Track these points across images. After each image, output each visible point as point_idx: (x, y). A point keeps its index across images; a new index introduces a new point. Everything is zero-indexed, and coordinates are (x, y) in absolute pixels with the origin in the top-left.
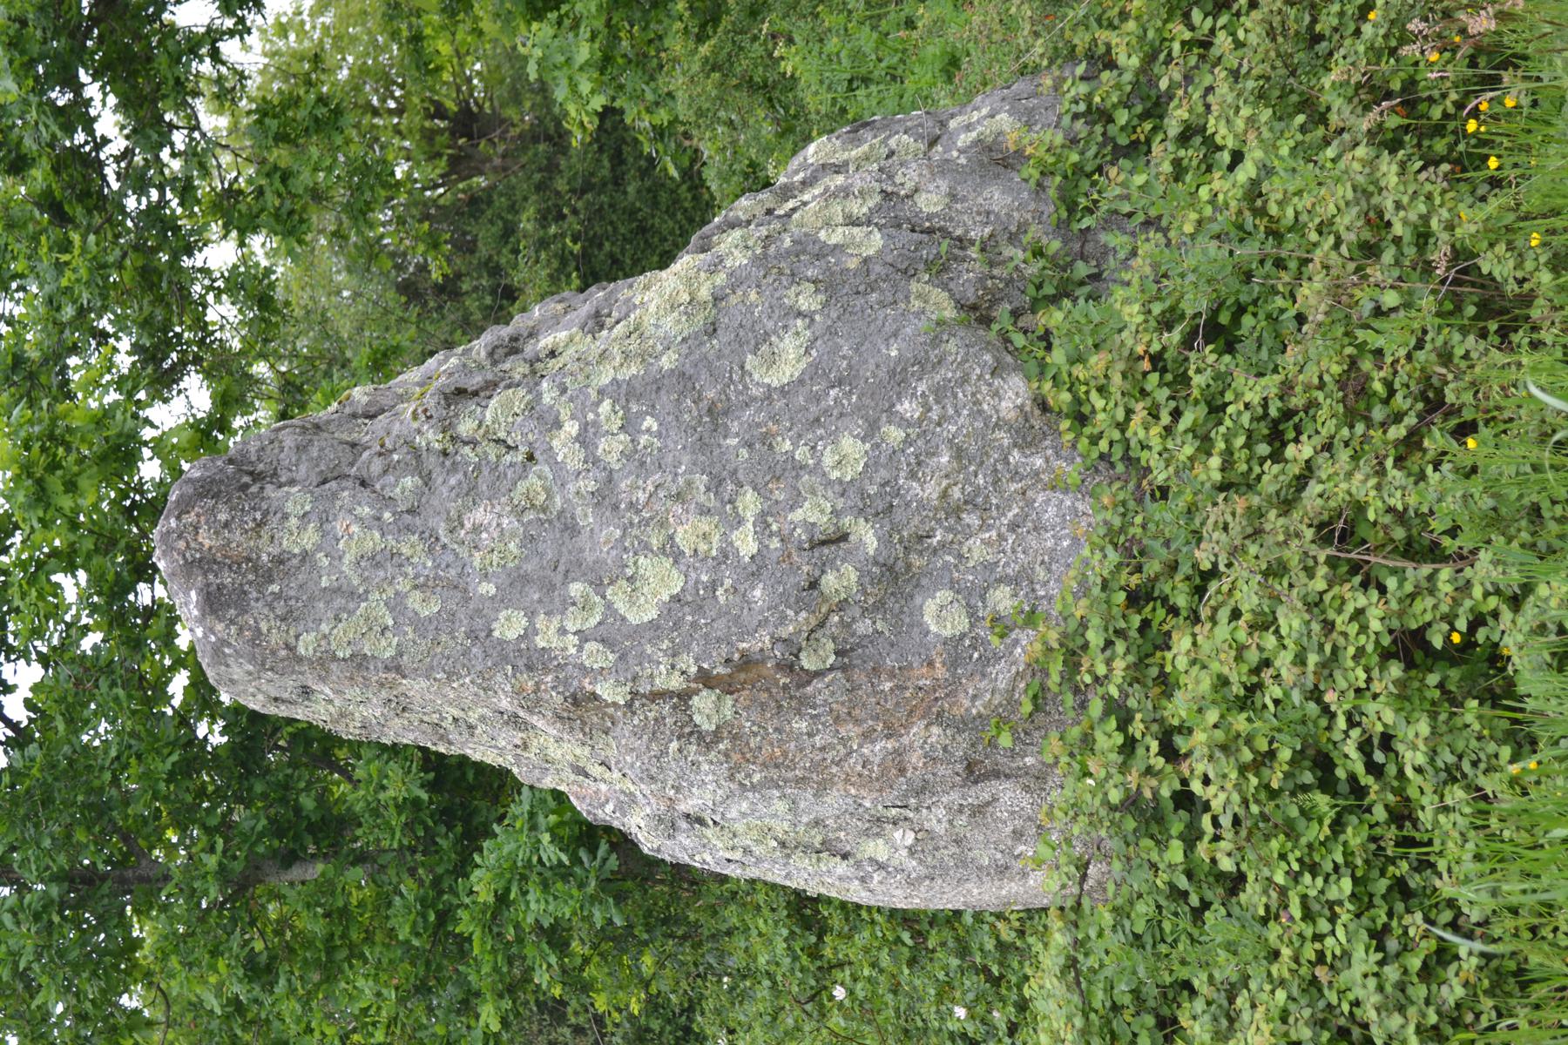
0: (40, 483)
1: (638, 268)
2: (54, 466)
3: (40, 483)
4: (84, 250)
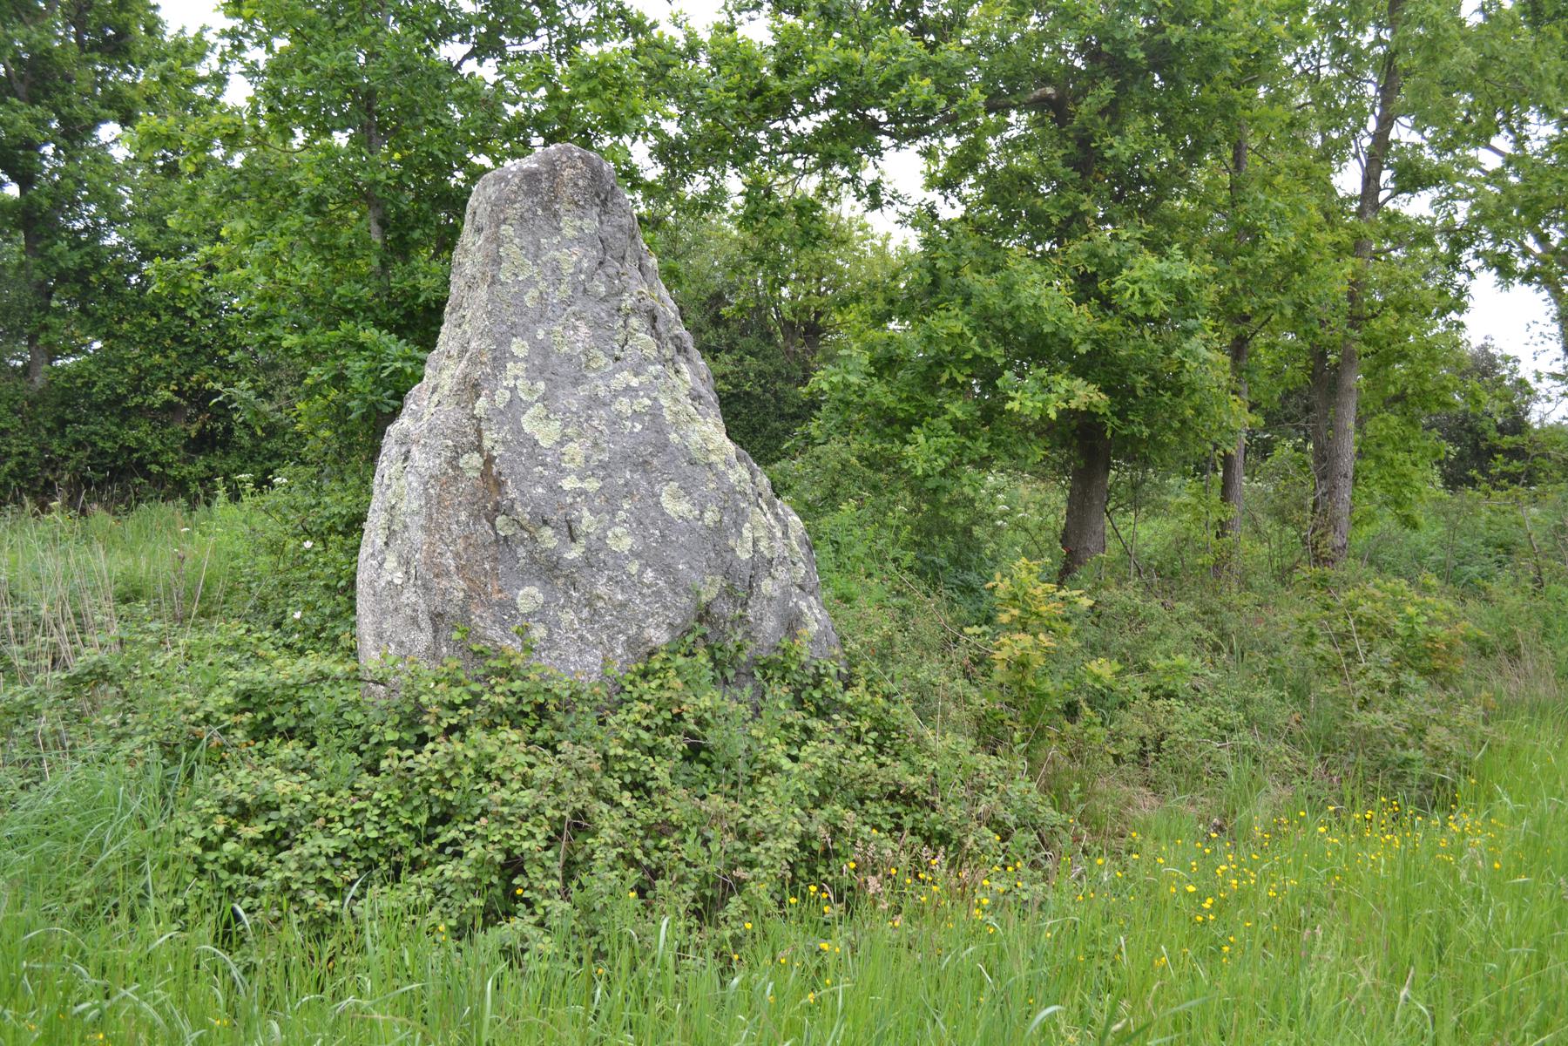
0: (595, 76)
1: (724, 415)
2: (606, 86)
3: (595, 76)
4: (728, 99)
